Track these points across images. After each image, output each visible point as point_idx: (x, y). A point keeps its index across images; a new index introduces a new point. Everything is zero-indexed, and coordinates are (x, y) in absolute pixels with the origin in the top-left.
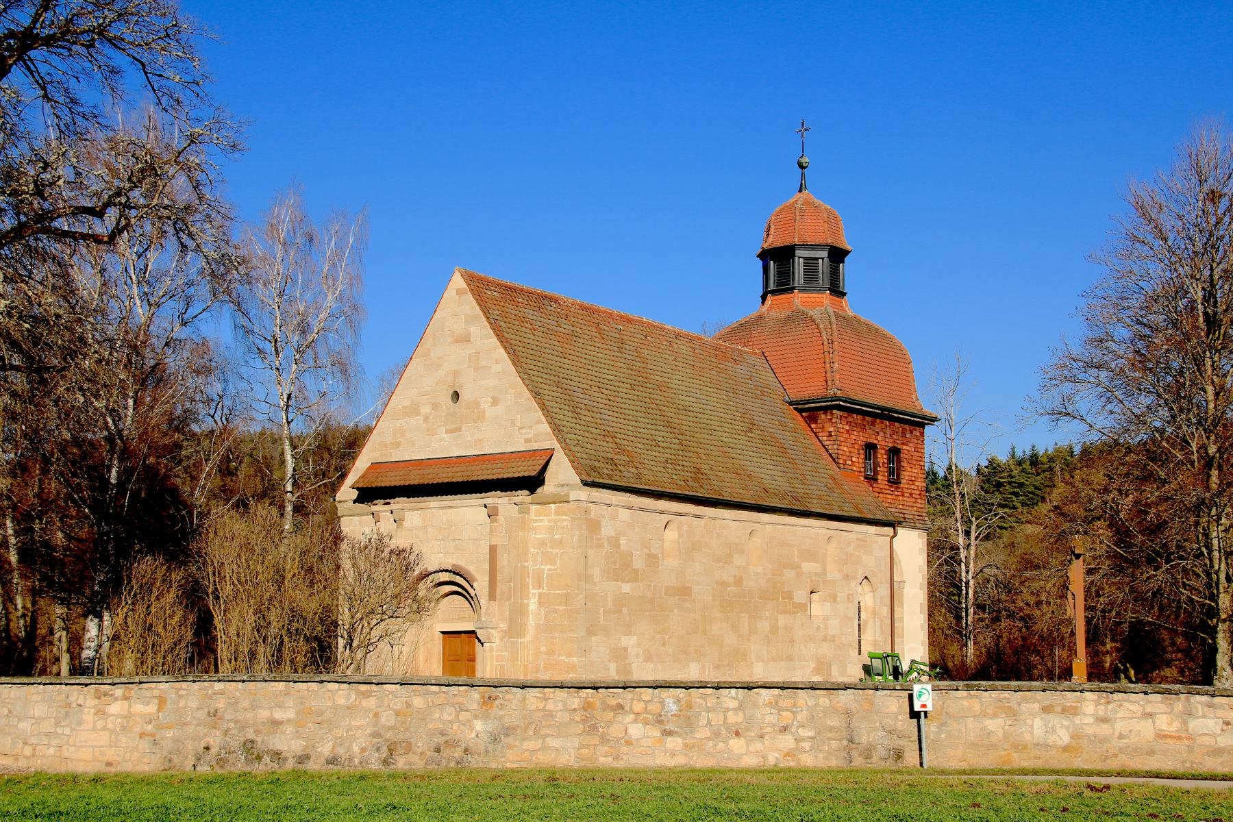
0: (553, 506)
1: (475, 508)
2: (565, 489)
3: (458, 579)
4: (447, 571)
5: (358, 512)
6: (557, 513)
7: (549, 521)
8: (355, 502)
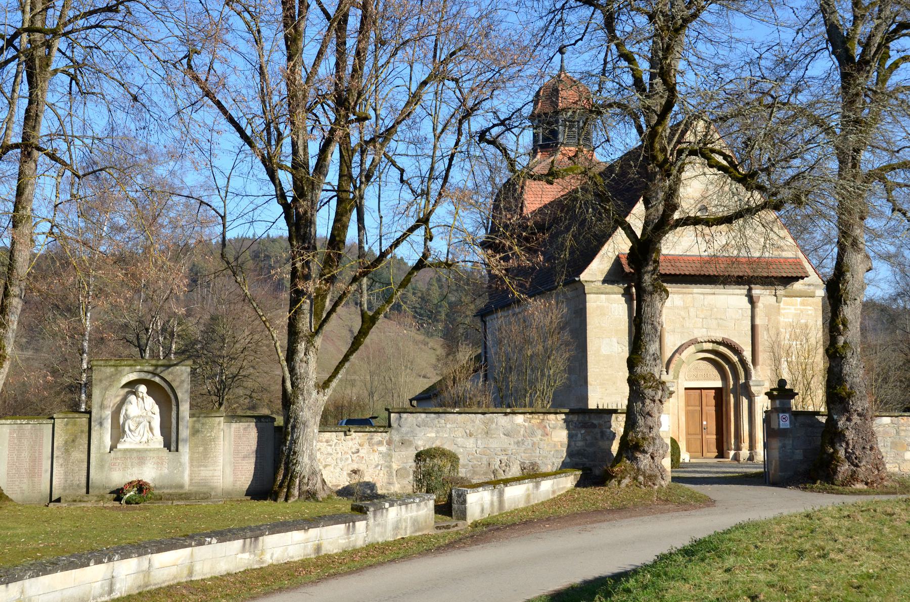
0: (799, 299)
1: (736, 296)
2: (812, 287)
3: (722, 349)
4: (709, 342)
5: (607, 290)
6: (802, 304)
7: (795, 309)
8: (604, 282)
